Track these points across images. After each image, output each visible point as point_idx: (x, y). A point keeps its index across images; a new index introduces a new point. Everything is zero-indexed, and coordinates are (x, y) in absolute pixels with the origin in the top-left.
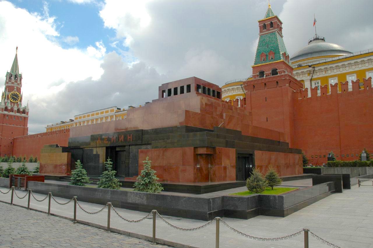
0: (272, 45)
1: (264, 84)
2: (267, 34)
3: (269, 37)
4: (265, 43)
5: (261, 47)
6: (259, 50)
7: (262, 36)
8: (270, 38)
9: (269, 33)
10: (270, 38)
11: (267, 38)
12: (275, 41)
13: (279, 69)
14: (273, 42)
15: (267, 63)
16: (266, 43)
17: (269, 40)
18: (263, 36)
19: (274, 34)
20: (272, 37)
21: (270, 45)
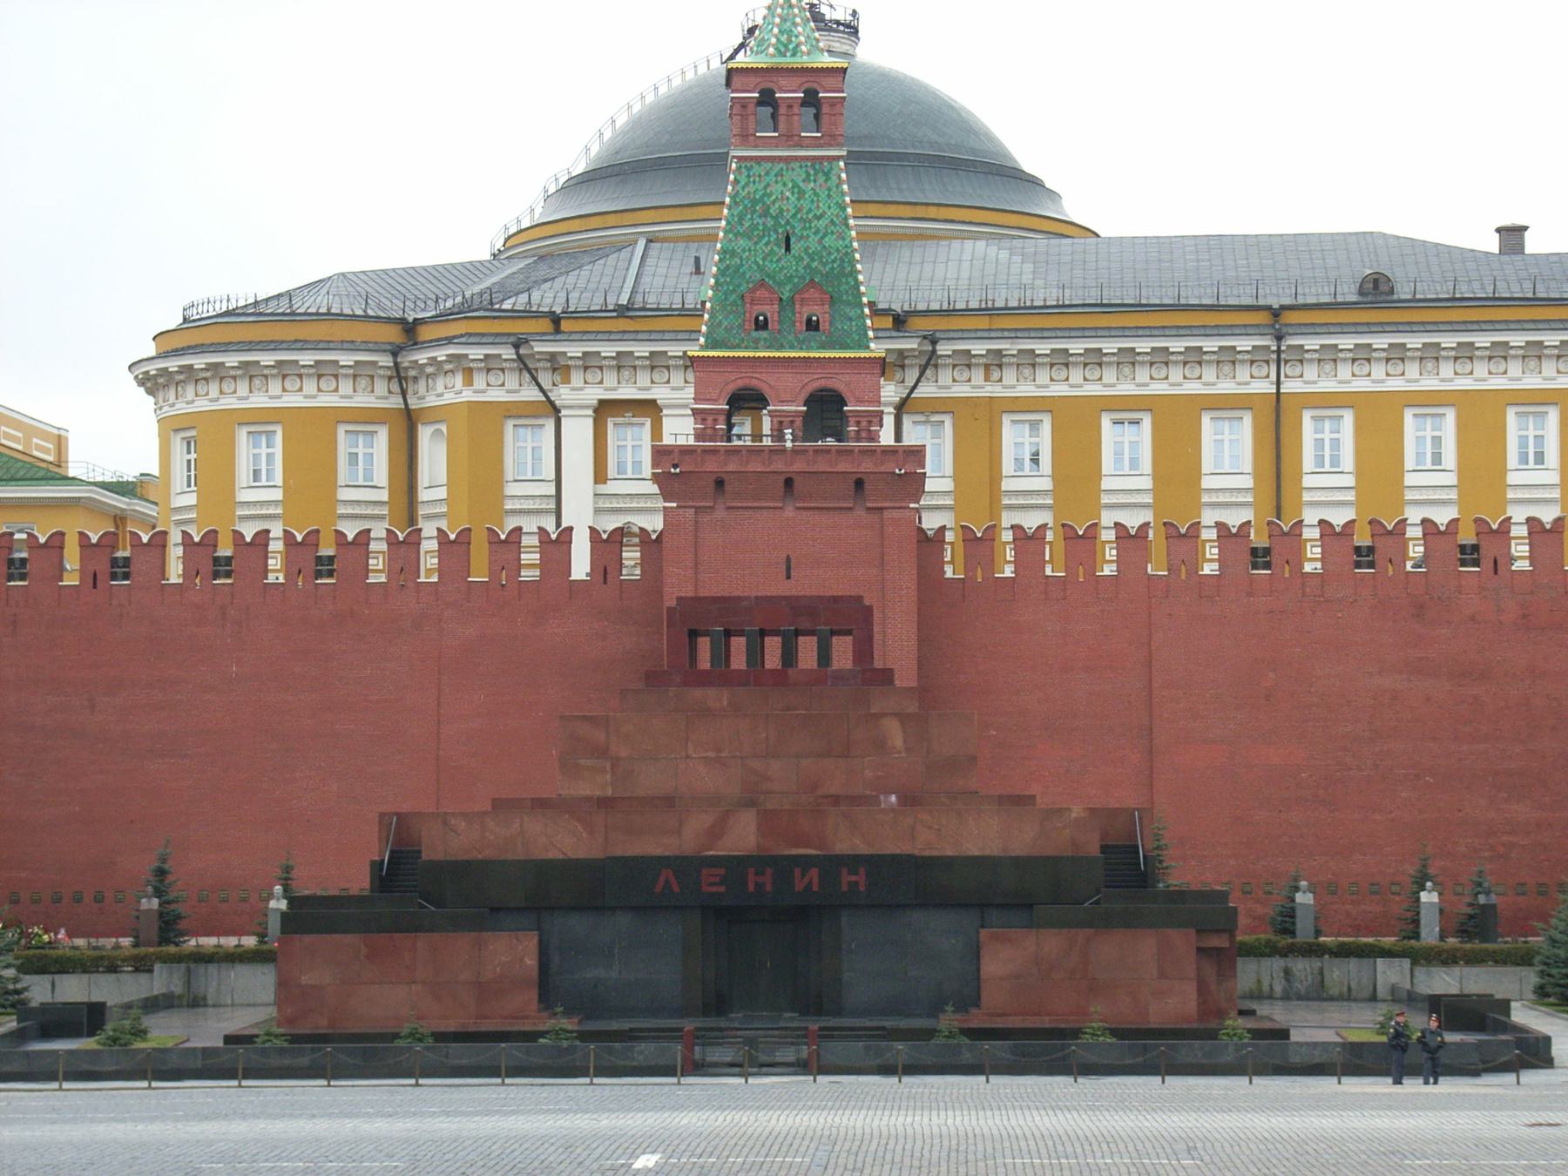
0: (813, 242)
1: (782, 478)
2: (782, 165)
3: (795, 185)
4: (770, 222)
5: (747, 235)
6: (733, 254)
7: (749, 169)
8: (801, 194)
9: (796, 158)
10: (801, 194)
11: (779, 187)
12: (832, 222)
13: (860, 402)
14: (822, 223)
15: (781, 347)
16: (777, 224)
17: (799, 210)
18: (757, 169)
19: (827, 175)
20: (816, 194)
21: (802, 237)
